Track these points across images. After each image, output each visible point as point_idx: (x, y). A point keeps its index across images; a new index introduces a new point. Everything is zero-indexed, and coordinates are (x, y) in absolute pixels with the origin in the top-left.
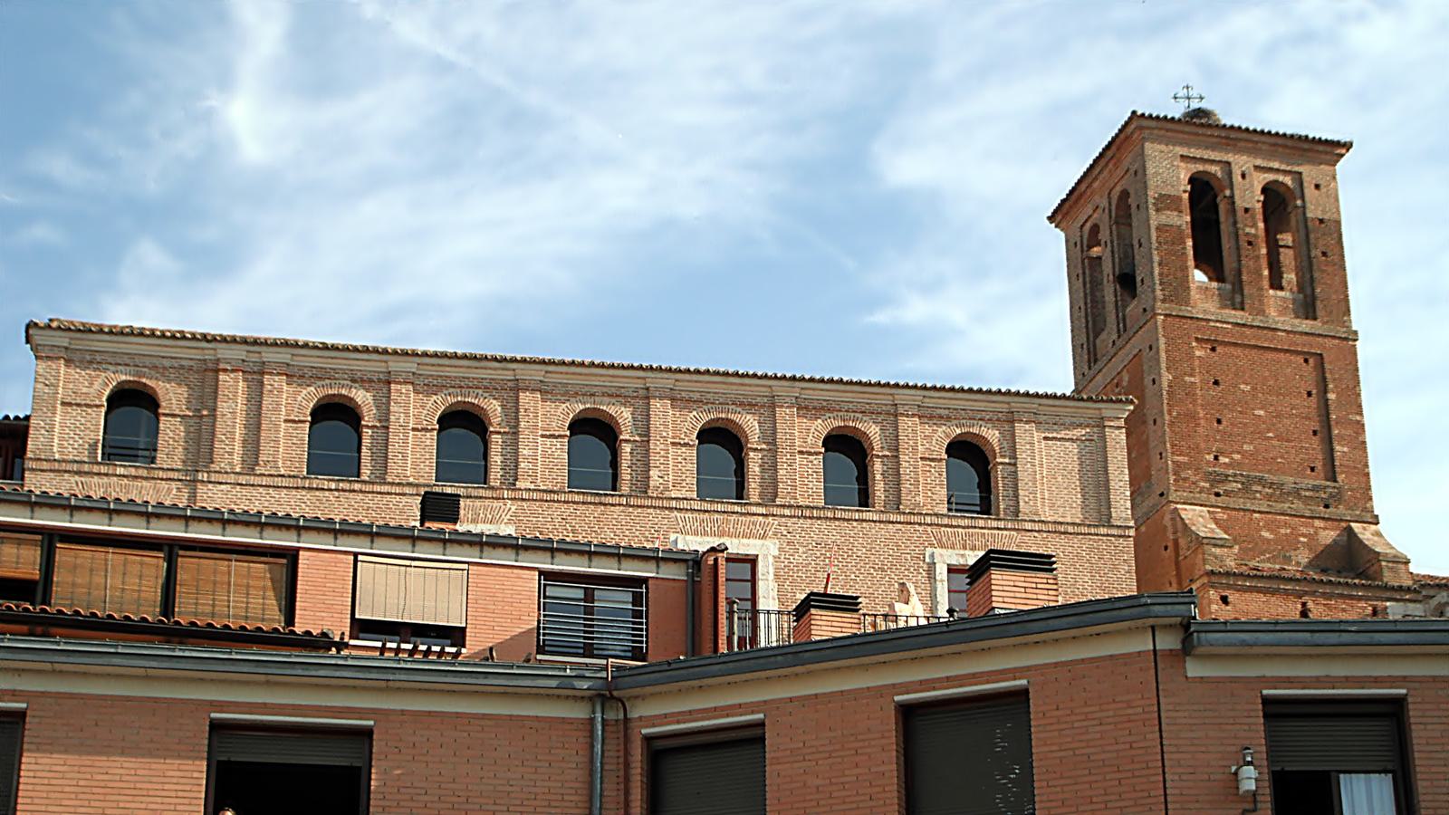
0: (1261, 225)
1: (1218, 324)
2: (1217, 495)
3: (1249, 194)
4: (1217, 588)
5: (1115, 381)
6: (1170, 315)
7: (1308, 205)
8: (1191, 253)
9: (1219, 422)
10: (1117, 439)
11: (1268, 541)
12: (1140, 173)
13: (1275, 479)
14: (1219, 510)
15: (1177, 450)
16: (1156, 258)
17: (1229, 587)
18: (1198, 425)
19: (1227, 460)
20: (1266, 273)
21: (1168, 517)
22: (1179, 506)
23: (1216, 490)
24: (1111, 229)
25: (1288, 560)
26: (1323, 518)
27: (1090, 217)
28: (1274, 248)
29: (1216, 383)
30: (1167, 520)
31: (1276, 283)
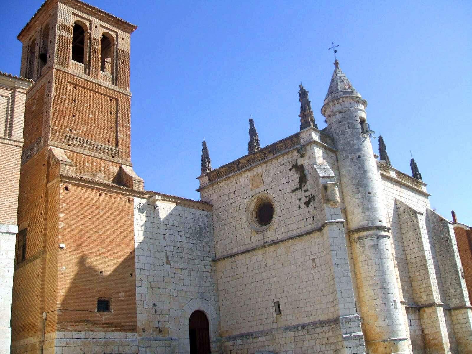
0: (100, 47)
1: (78, 78)
2: (69, 145)
3: (97, 34)
4: (64, 183)
5: (33, 97)
6: (59, 70)
7: (119, 44)
8: (71, 53)
9: (74, 116)
10: (21, 99)
11: (88, 167)
12: (54, 16)
13: (93, 142)
14: (69, 152)
15: (54, 124)
16: (56, 47)
17: (69, 183)
18: (65, 116)
19: (75, 132)
20: (100, 64)
21: (46, 153)
22: (52, 147)
23: (69, 143)
24: (40, 39)
25: (95, 176)
26: (111, 161)
27: (33, 36)
28: (103, 62)
29: (75, 101)
30: (46, 153)
31: (103, 69)
